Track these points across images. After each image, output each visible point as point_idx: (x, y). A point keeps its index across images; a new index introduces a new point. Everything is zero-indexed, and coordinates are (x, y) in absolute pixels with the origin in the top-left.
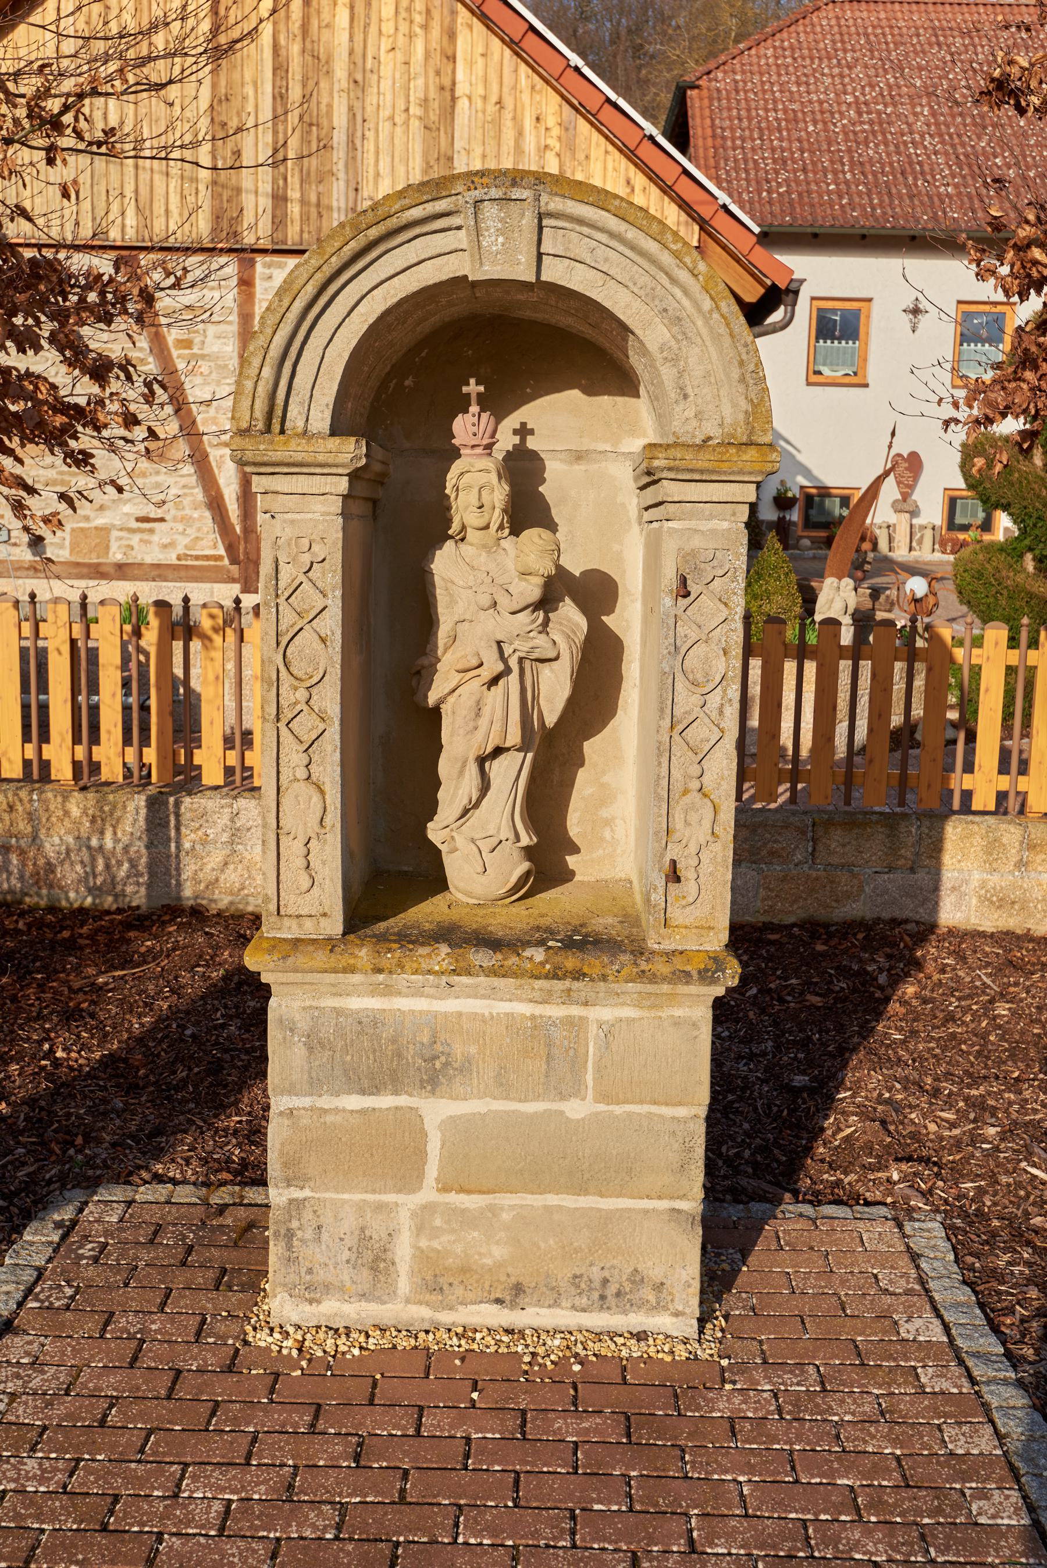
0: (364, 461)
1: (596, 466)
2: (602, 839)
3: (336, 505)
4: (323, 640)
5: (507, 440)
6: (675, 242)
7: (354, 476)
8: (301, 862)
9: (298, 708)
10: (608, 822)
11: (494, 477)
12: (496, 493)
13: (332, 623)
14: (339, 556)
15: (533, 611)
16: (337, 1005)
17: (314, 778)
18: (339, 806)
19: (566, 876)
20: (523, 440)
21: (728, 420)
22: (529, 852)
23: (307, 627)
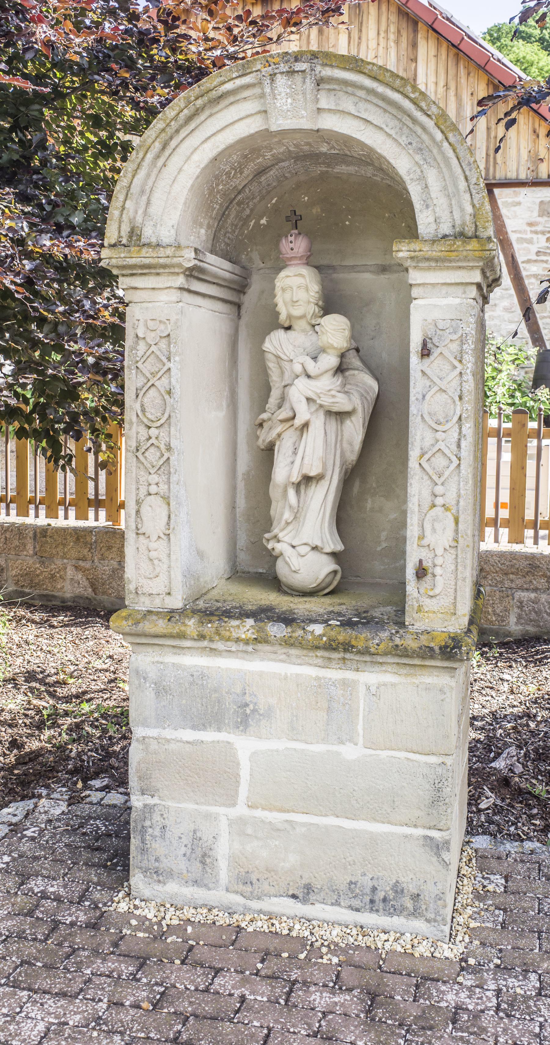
6: (413, 92)
16: (176, 662)
21: (458, 222)
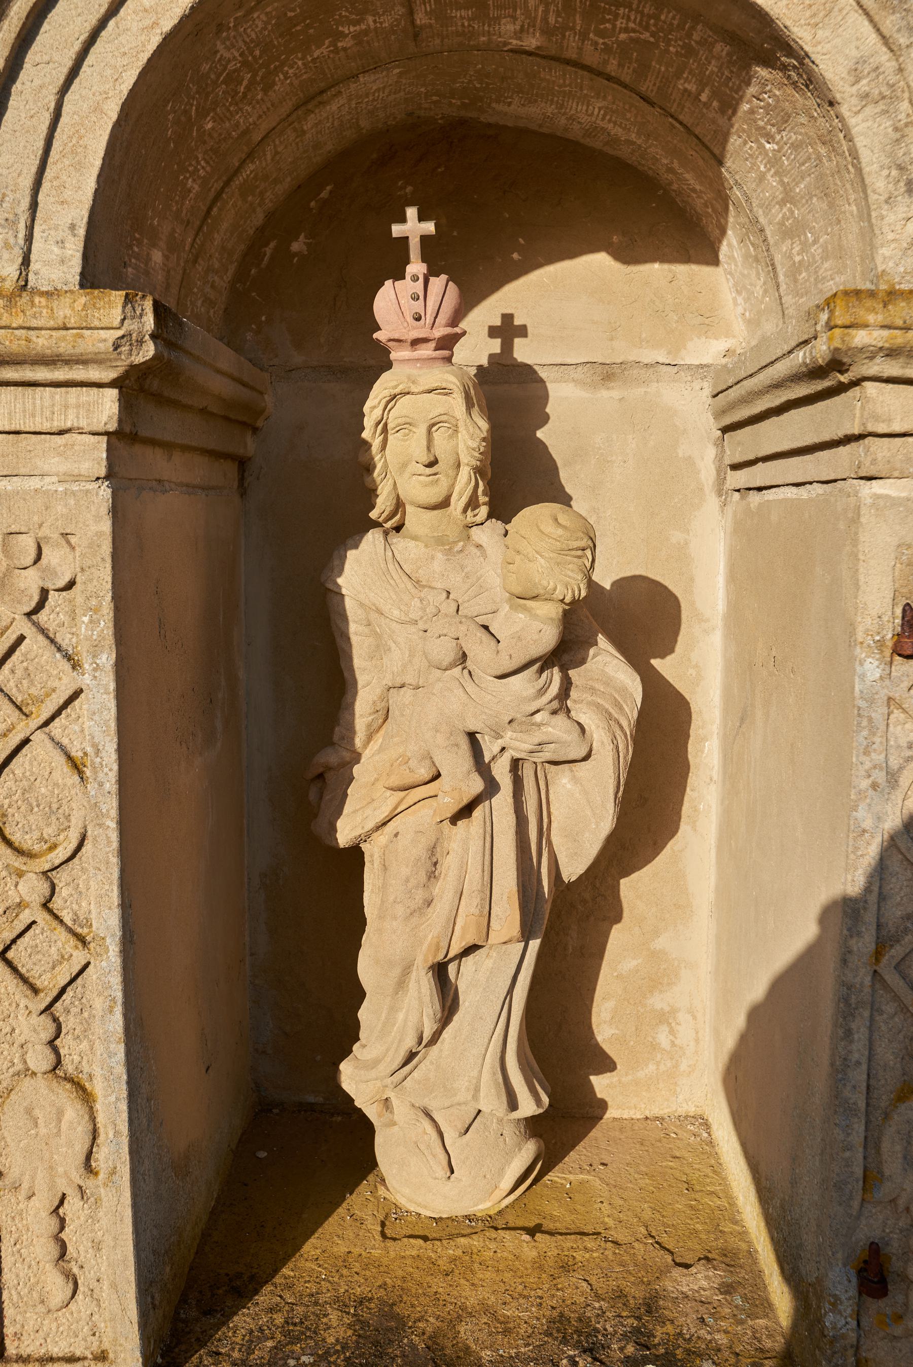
0: (149, 350)
1: (641, 391)
2: (654, 1047)
3: (93, 456)
4: (77, 766)
5: (476, 349)
7: (134, 386)
8: (45, 1250)
9: (26, 917)
10: (664, 1018)
11: (457, 404)
12: (463, 434)
13: (95, 727)
14: (105, 574)
15: (541, 671)
17: (69, 1066)
18: (124, 1128)
19: (590, 1112)
20: (507, 347)
22: (533, 1126)
23: (39, 737)
